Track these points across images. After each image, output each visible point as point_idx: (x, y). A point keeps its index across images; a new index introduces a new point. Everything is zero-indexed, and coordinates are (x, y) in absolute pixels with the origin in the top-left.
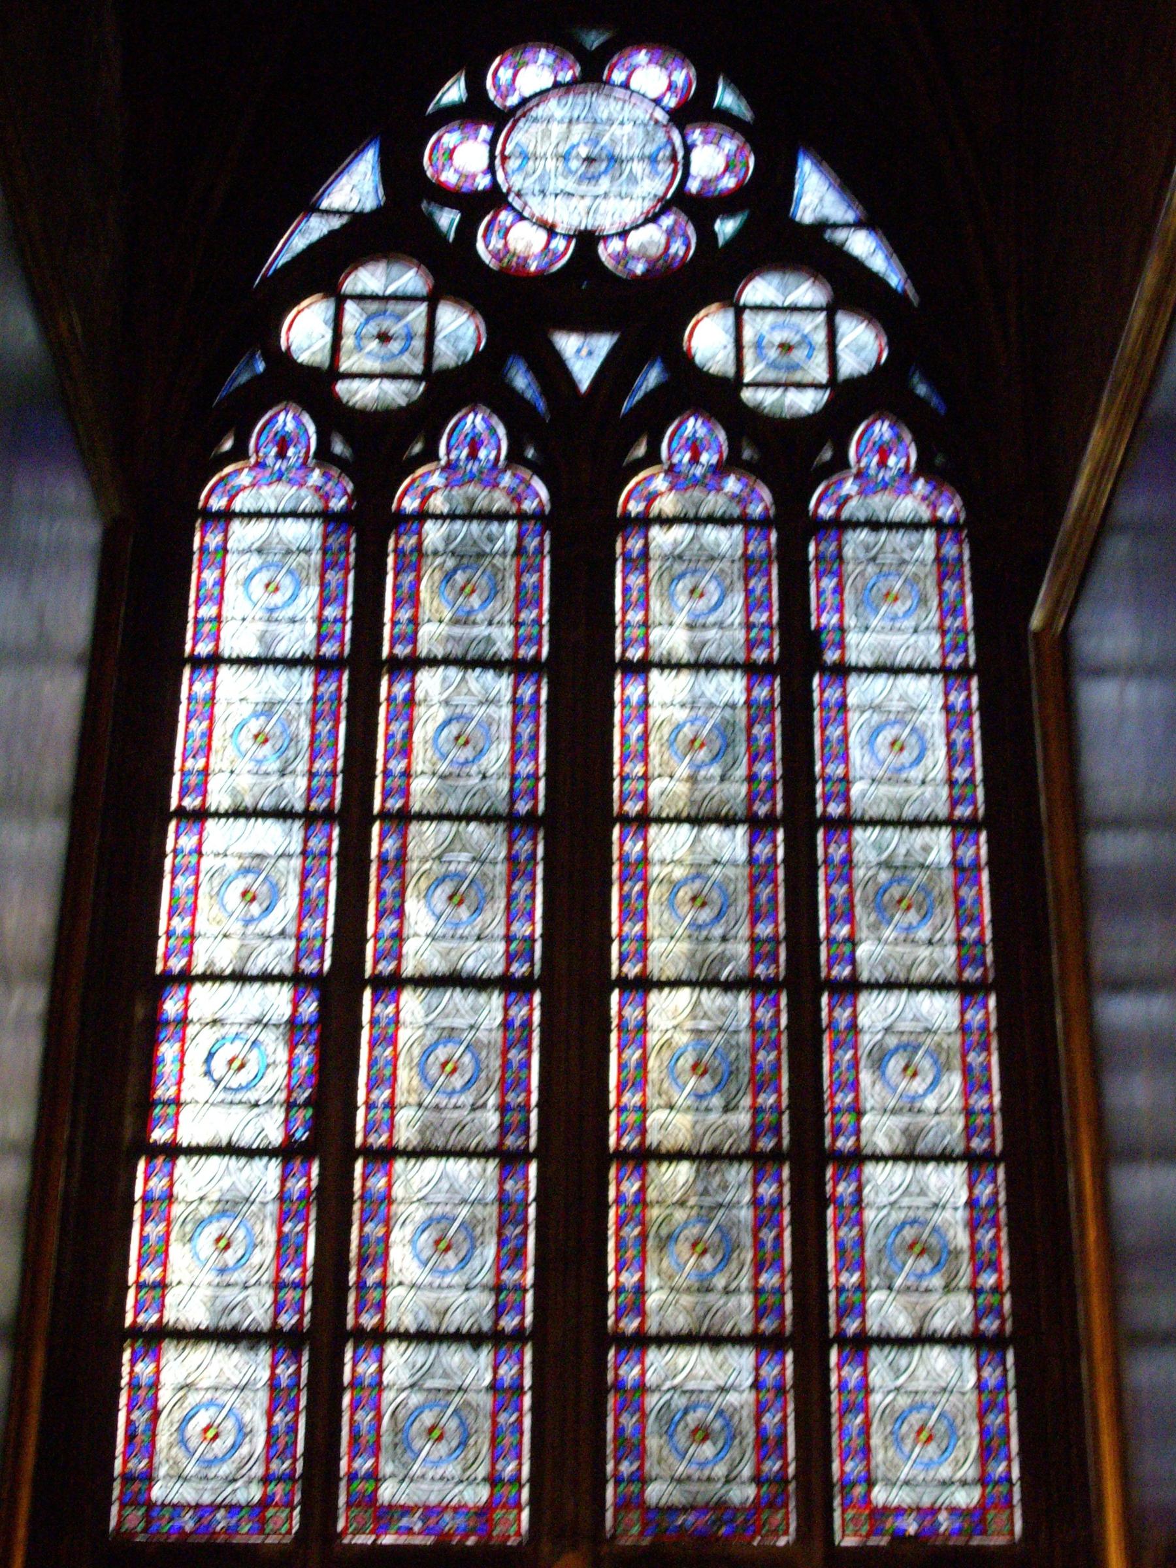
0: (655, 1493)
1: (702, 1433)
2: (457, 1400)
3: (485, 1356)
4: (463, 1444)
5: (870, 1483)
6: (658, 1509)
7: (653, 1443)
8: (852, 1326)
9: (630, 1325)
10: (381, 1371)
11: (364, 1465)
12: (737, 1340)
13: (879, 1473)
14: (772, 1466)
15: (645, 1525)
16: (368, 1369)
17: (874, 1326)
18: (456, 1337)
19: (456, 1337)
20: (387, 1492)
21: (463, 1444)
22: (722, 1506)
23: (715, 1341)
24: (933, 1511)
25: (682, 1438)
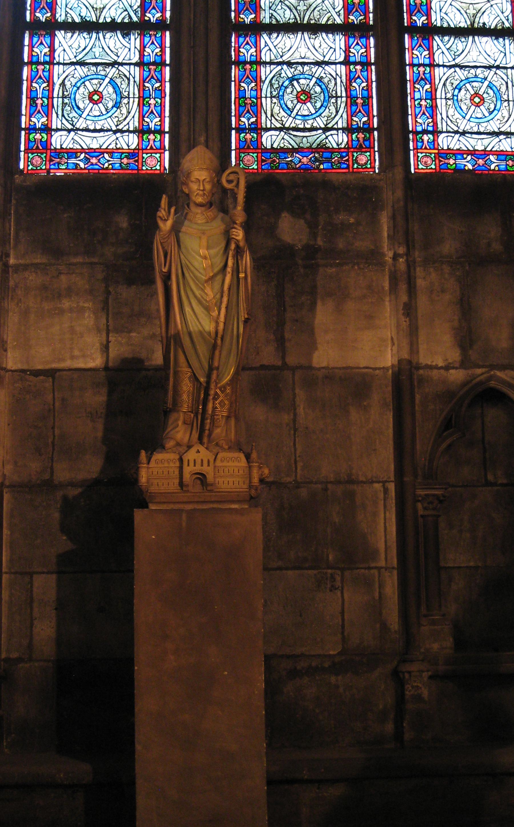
0: (268, 139)
1: (304, 96)
2: (112, 72)
3: (135, 40)
4: (117, 105)
5: (436, 132)
6: (273, 150)
7: (267, 103)
8: (420, 20)
9: (248, 18)
10: (52, 50)
11: (39, 121)
12: (331, 28)
13: (442, 126)
14: (360, 120)
15: (261, 162)
16: (41, 51)
17: (436, 20)
18: (112, 26)
19: (112, 26)
20: (58, 140)
21: (117, 105)
22: (322, 148)
23: (315, 29)
24: (485, 153)
25: (289, 98)
